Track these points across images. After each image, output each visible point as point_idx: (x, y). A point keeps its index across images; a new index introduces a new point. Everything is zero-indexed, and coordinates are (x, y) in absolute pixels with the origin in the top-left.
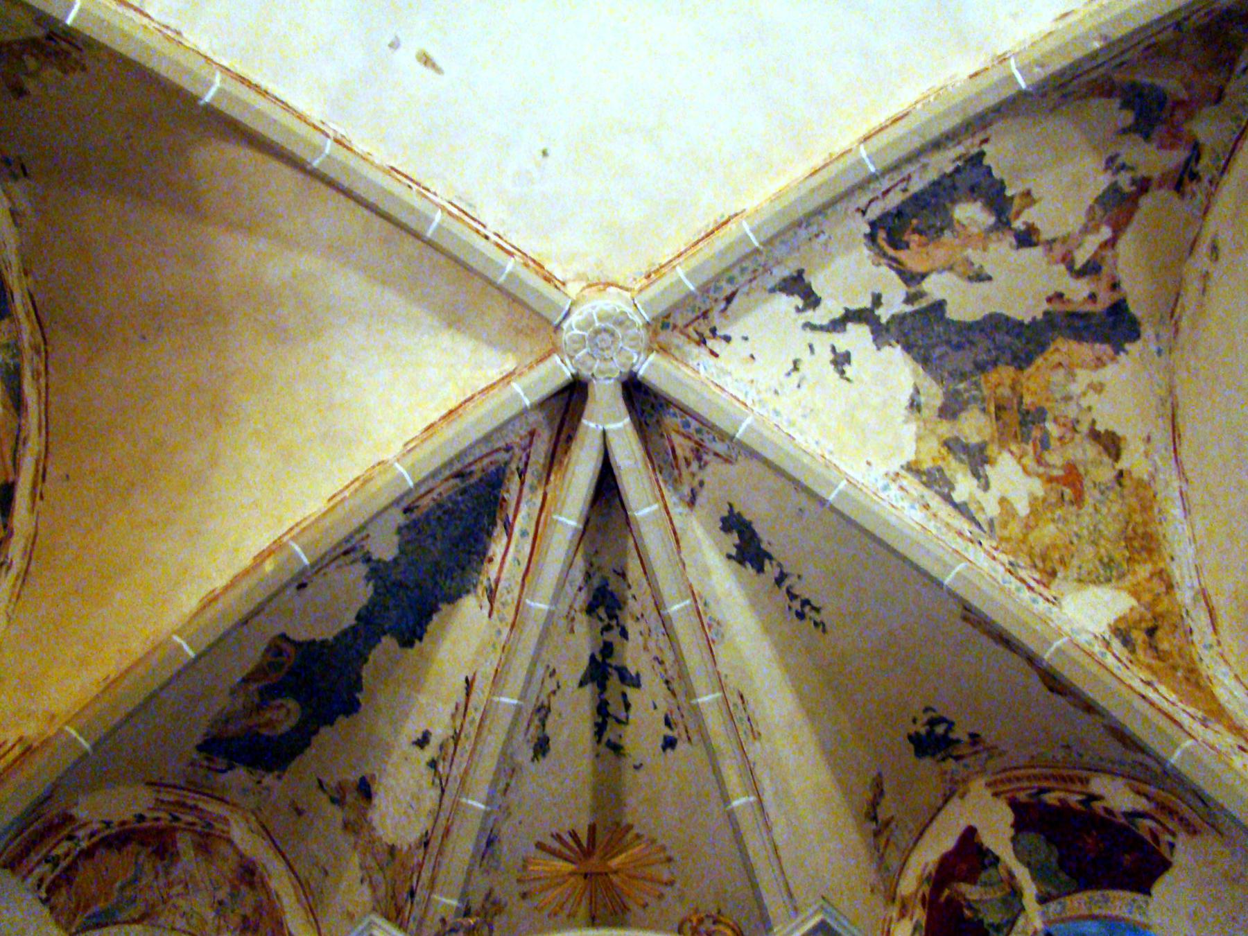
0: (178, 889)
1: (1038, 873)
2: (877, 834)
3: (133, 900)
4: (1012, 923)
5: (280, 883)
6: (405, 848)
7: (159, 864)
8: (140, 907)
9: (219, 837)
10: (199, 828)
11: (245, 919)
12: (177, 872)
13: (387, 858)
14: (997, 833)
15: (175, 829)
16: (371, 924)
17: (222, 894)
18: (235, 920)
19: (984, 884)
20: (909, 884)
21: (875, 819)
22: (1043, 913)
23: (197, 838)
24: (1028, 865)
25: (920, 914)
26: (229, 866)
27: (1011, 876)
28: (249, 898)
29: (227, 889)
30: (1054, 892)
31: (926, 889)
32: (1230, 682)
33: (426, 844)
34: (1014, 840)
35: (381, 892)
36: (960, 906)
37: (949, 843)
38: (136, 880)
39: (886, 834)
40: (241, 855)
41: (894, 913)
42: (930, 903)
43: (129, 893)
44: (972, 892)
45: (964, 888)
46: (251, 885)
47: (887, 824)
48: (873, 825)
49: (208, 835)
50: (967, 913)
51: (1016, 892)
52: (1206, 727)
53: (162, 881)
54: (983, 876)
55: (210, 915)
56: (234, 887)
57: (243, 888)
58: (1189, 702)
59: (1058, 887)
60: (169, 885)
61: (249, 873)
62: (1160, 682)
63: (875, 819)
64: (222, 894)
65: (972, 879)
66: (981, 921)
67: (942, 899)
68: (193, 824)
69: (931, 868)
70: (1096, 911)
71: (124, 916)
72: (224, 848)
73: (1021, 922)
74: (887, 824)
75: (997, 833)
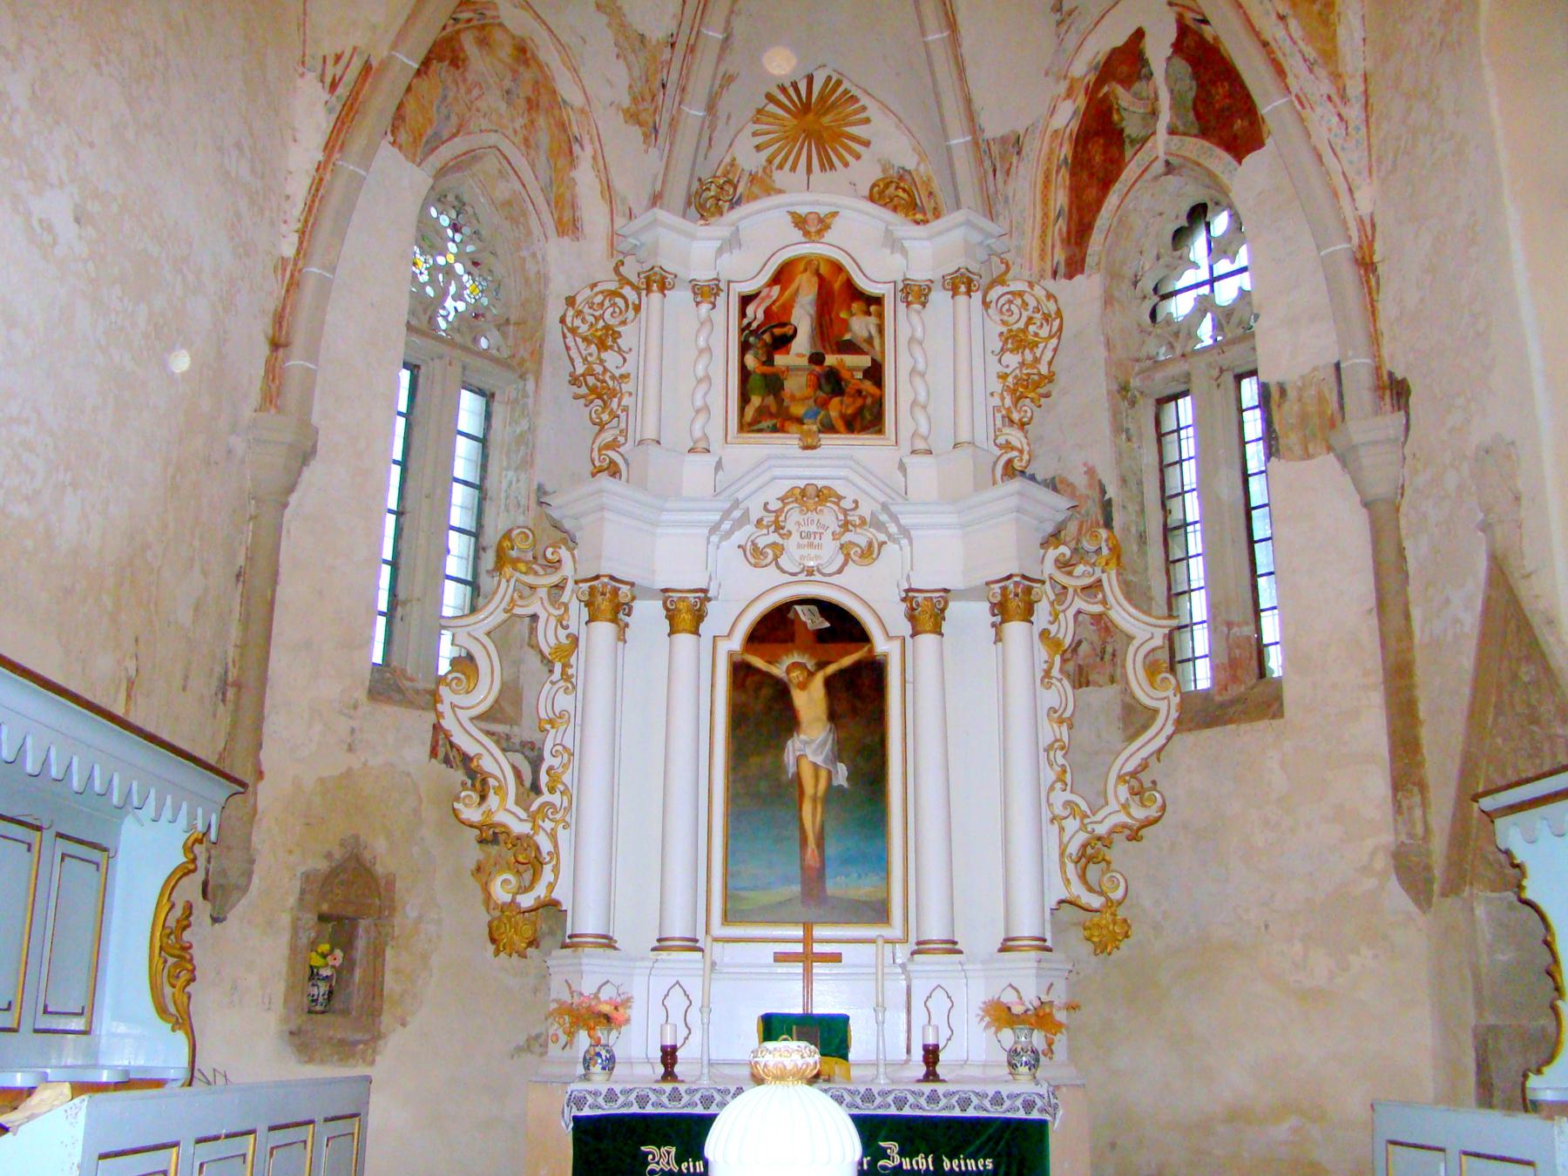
0: (475, 93)
1: (1176, 104)
2: (1059, 23)
3: (448, 118)
4: (1144, 140)
5: (548, 55)
6: (654, 42)
7: (457, 73)
8: (454, 120)
9: (492, 25)
10: (475, 23)
11: (529, 100)
12: (470, 77)
13: (637, 45)
14: (1158, 50)
15: (458, 32)
16: (655, 222)
17: (507, 83)
18: (522, 103)
19: (1136, 95)
20: (1082, 68)
21: (1060, 10)
22: (1167, 143)
23: (476, 32)
24: (1172, 92)
25: (1081, 100)
26: (506, 52)
27: (1156, 98)
28: (527, 75)
29: (509, 76)
30: (1181, 128)
31: (1092, 77)
32: (1356, 22)
33: (673, 45)
34: (1169, 59)
35: (636, 73)
36: (1110, 108)
37: (1119, 39)
38: (445, 97)
39: (1069, 21)
40: (513, 37)
41: (1063, 87)
42: (1091, 92)
43: (444, 111)
44: (1123, 97)
45: (1120, 90)
46: (526, 63)
47: (1070, 14)
48: (1058, 16)
49: (483, 27)
50: (1115, 117)
51: (1154, 114)
52: (1311, 71)
53: (463, 90)
54: (1137, 86)
55: (503, 106)
56: (515, 72)
57: (522, 69)
58: (1309, 39)
59: (1185, 124)
60: (469, 91)
61: (523, 52)
62: (1296, 16)
63: (1060, 10)
64: (507, 83)
65: (1127, 82)
66: (1122, 131)
67: (1101, 95)
68: (469, 20)
69: (1101, 58)
70: (1201, 161)
71: (445, 135)
72: (498, 35)
73: (1149, 144)
74: (1070, 14)
75: (1158, 50)
